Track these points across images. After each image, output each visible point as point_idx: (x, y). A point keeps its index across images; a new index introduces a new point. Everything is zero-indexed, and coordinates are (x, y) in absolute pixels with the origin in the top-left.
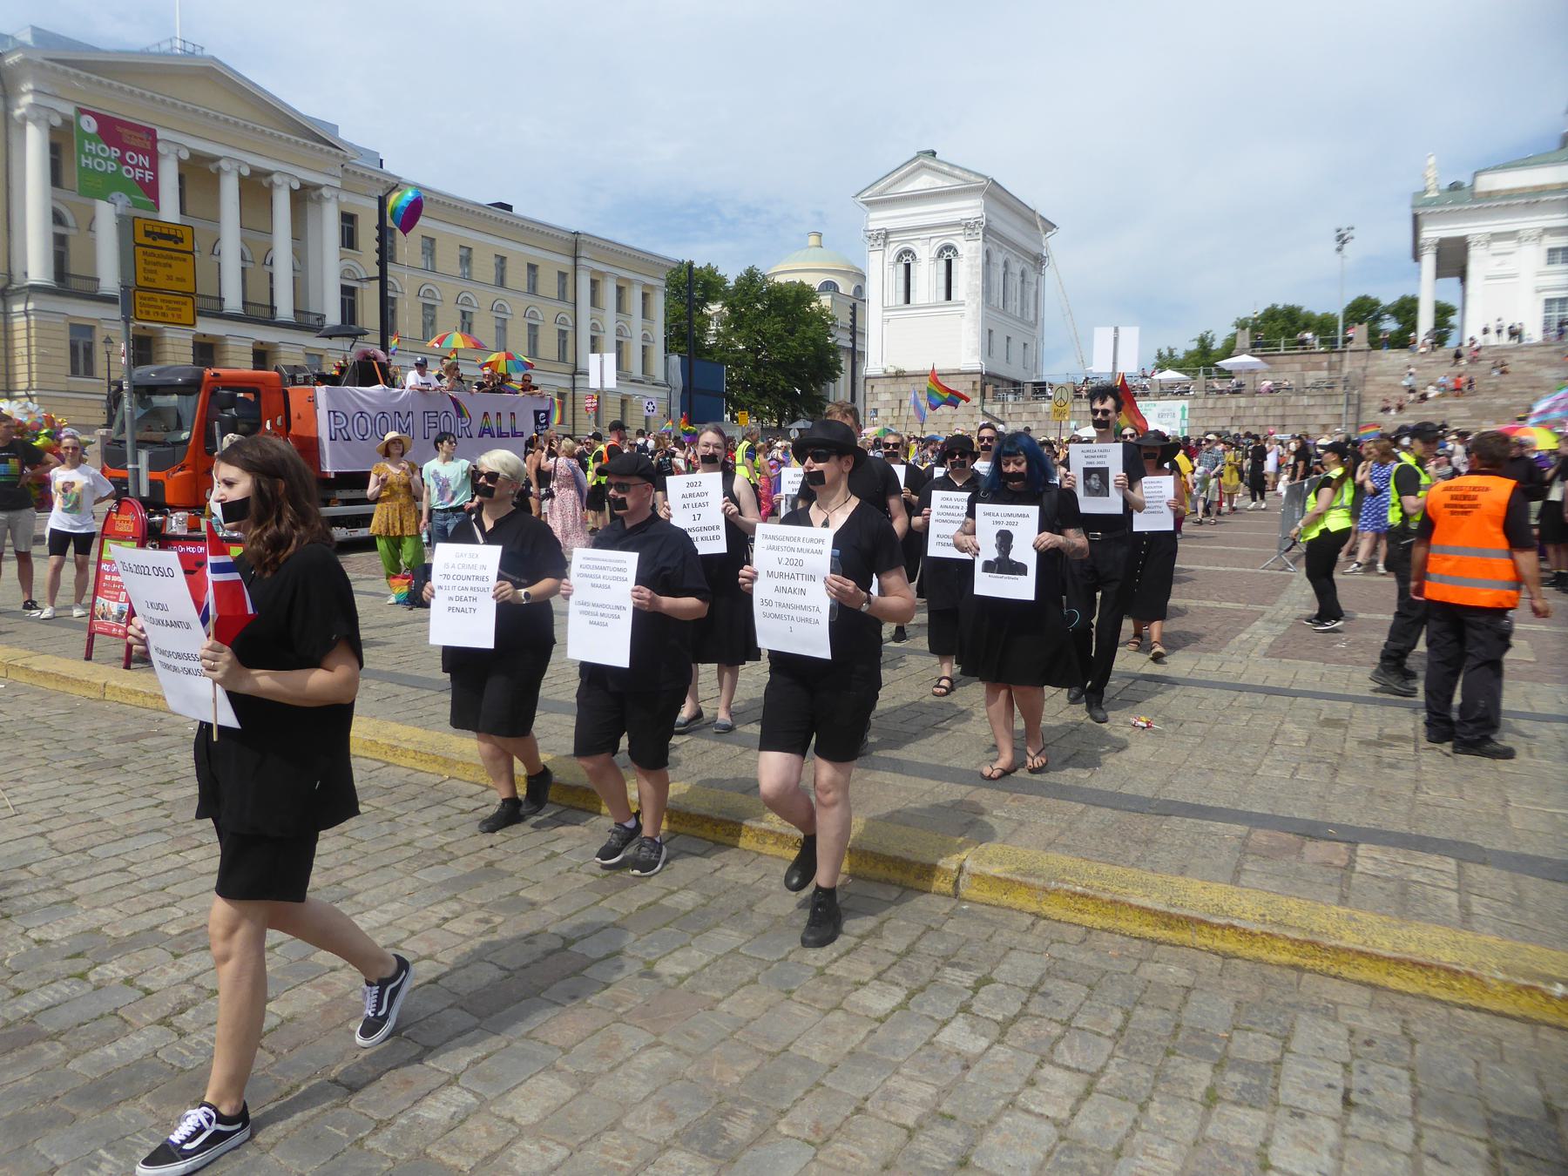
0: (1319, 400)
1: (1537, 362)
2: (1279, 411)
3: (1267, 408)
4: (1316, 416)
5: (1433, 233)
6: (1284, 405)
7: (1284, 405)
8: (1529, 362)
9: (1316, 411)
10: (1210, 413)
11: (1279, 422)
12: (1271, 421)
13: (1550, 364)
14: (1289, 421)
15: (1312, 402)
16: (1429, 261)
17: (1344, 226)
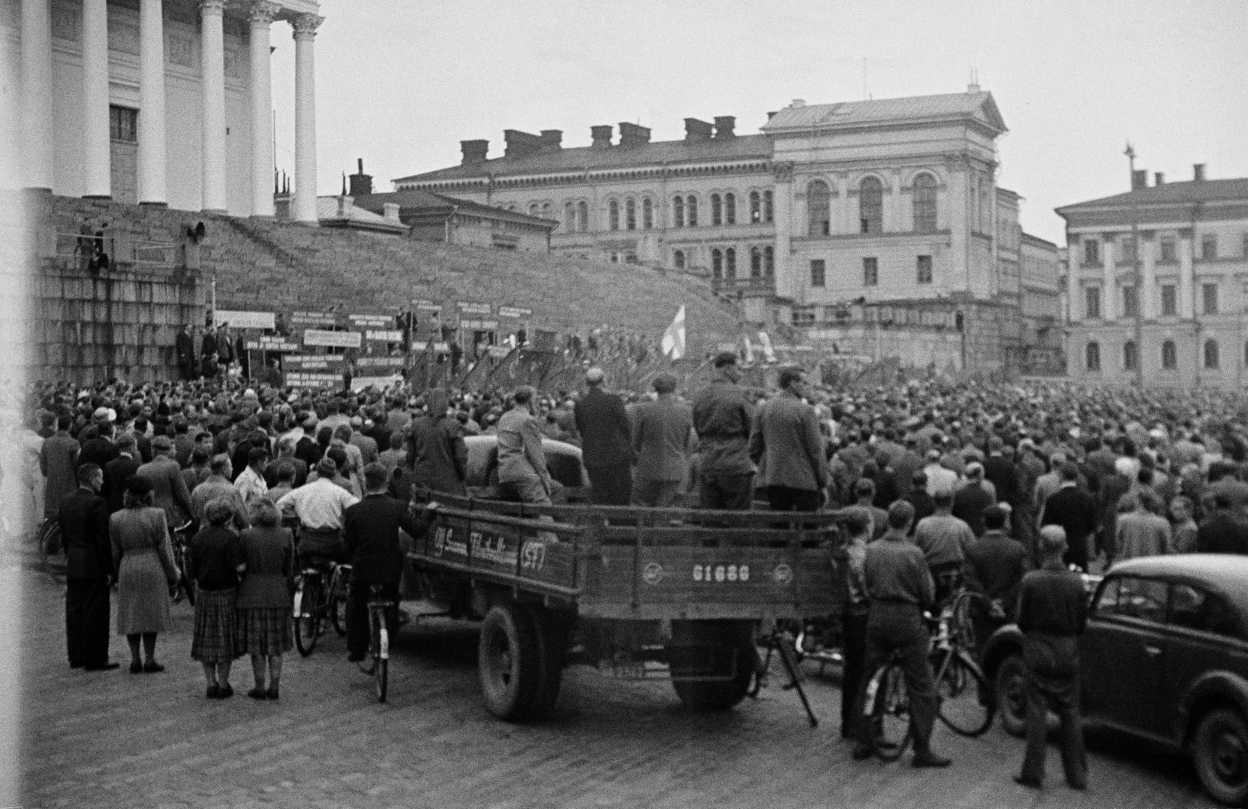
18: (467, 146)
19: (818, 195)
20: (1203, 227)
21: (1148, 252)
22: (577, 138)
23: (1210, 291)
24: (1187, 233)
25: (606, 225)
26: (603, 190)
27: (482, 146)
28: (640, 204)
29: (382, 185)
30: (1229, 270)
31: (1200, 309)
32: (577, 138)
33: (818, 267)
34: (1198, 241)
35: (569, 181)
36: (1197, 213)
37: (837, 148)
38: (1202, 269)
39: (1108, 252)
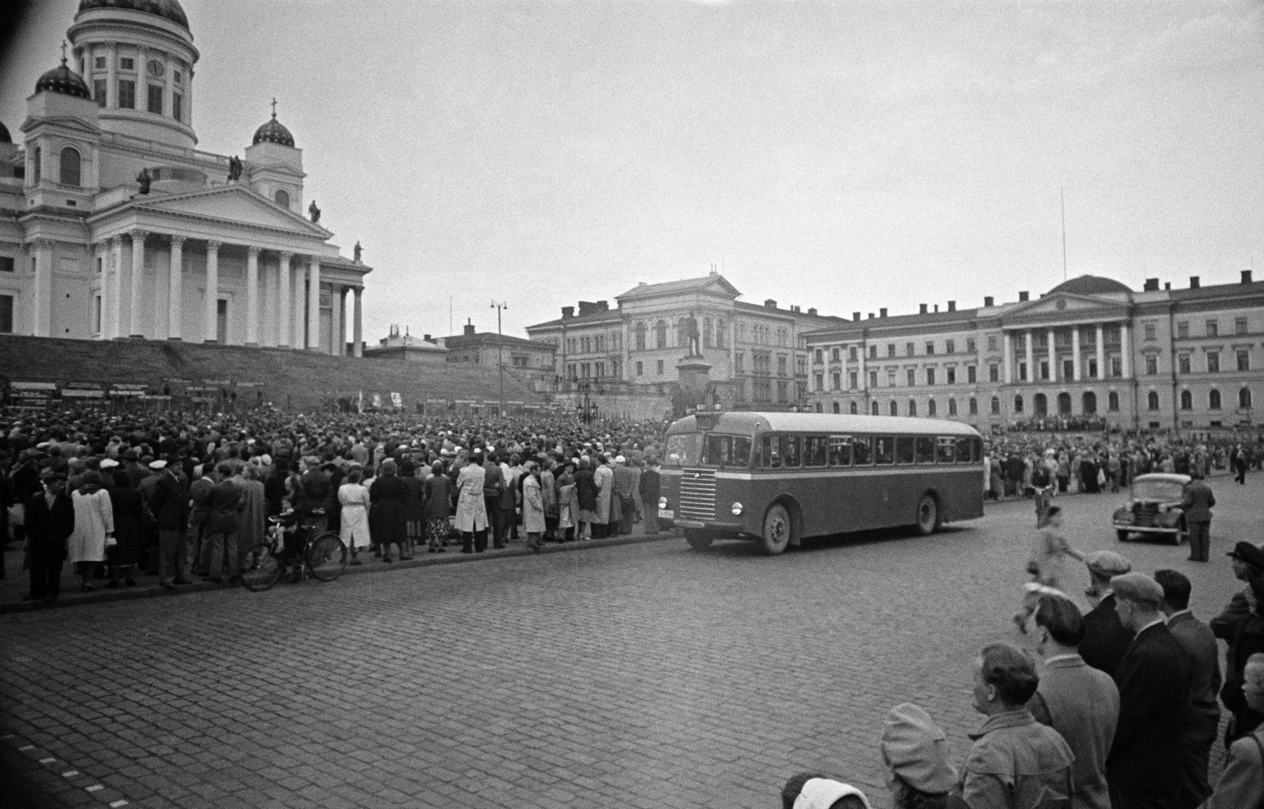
19: (641, 329)
20: (871, 342)
21: (844, 355)
23: (874, 375)
24: (863, 345)
26: (610, 330)
27: (571, 309)
29: (478, 331)
30: (883, 364)
31: (869, 384)
32: (613, 305)
33: (640, 365)
34: (868, 349)
35: (597, 326)
36: (866, 334)
37: (648, 306)
38: (869, 364)
39: (826, 355)
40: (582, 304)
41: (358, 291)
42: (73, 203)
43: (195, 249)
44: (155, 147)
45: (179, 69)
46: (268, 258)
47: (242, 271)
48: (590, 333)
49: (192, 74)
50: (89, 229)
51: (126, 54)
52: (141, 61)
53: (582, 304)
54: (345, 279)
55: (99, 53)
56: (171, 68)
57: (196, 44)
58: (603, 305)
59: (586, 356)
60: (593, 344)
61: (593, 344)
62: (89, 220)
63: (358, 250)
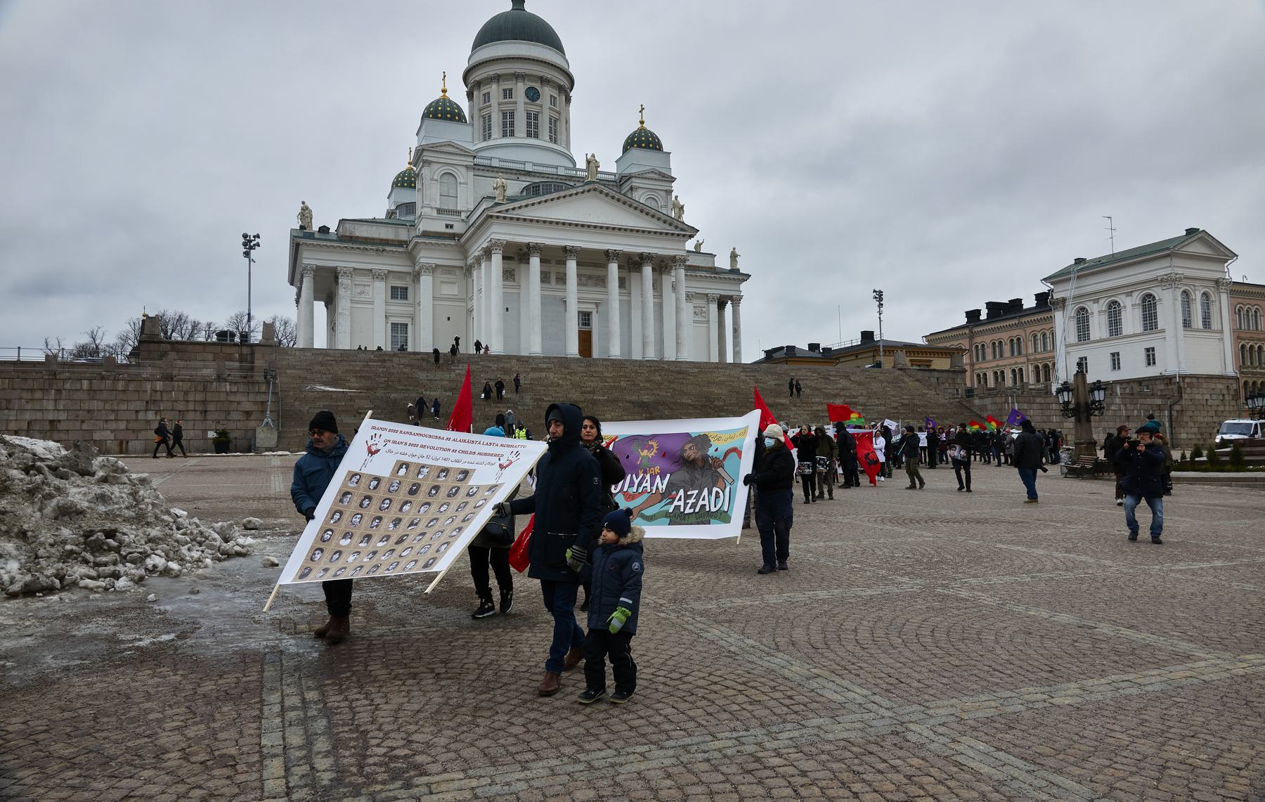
0: (242, 388)
1: (412, 366)
2: (199, 397)
3: (186, 393)
4: (239, 403)
5: (311, 259)
6: (205, 390)
7: (205, 390)
8: (406, 365)
9: (239, 398)
10: (121, 396)
11: (199, 407)
12: (191, 406)
13: (420, 368)
14: (211, 407)
15: (234, 389)
16: (308, 283)
17: (251, 234)
18: (969, 314)
19: (1082, 320)
22: (1029, 303)
25: (1031, 350)
27: (977, 313)
28: (1039, 336)
40: (990, 306)
41: (736, 301)
42: (452, 227)
43: (554, 258)
44: (529, 168)
45: (555, 93)
46: (632, 263)
47: (602, 281)
48: (1005, 336)
49: (568, 100)
50: (463, 250)
51: (507, 85)
52: (520, 88)
53: (990, 306)
54: (722, 286)
55: (485, 90)
56: (547, 92)
57: (572, 70)
58: (1017, 303)
59: (1001, 363)
60: (1007, 348)
61: (1007, 348)
62: (463, 240)
63: (734, 256)
